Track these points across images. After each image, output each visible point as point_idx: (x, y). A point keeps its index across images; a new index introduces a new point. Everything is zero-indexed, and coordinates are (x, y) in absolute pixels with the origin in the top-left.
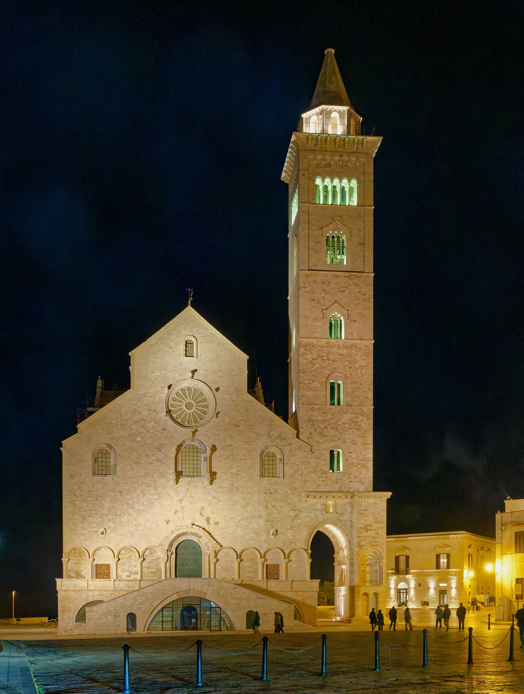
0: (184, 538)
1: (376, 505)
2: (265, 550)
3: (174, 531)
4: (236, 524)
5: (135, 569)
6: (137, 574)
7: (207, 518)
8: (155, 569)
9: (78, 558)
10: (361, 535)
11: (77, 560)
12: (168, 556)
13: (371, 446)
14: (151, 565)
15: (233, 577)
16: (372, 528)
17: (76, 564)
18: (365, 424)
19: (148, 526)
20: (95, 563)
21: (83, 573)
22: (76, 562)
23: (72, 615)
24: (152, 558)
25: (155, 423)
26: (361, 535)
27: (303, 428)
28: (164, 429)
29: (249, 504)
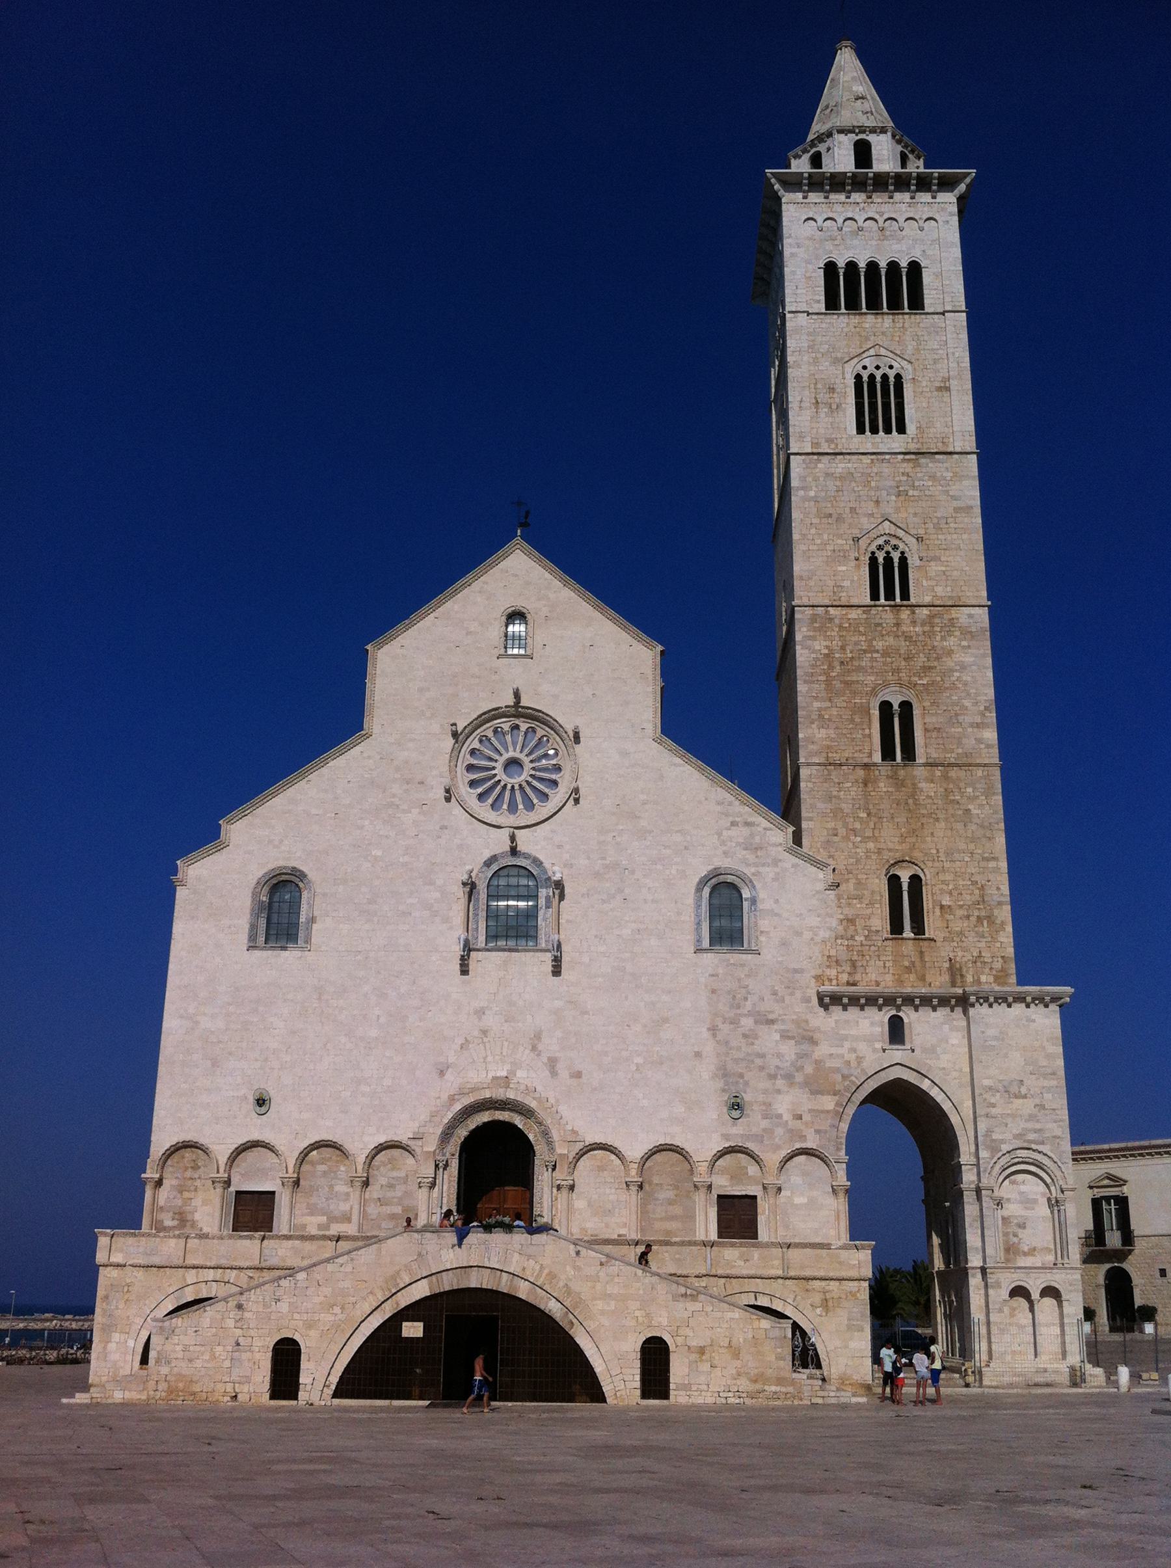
0: (485, 1117)
1: (1031, 1023)
2: (715, 1152)
3: (456, 1097)
4: (629, 1076)
5: (344, 1207)
6: (349, 1220)
7: (550, 1059)
8: (400, 1208)
9: (189, 1174)
10: (994, 1111)
11: (185, 1178)
12: (437, 1166)
13: (1004, 865)
14: (389, 1194)
15: (623, 1232)
16: (1023, 1090)
17: (181, 1192)
18: (981, 806)
19: (387, 1082)
20: (232, 1189)
21: (197, 1216)
22: (181, 1186)
23: (131, 1343)
24: (395, 1174)
25: (419, 813)
26: (994, 1111)
27: (811, 819)
28: (443, 828)
29: (665, 1020)
